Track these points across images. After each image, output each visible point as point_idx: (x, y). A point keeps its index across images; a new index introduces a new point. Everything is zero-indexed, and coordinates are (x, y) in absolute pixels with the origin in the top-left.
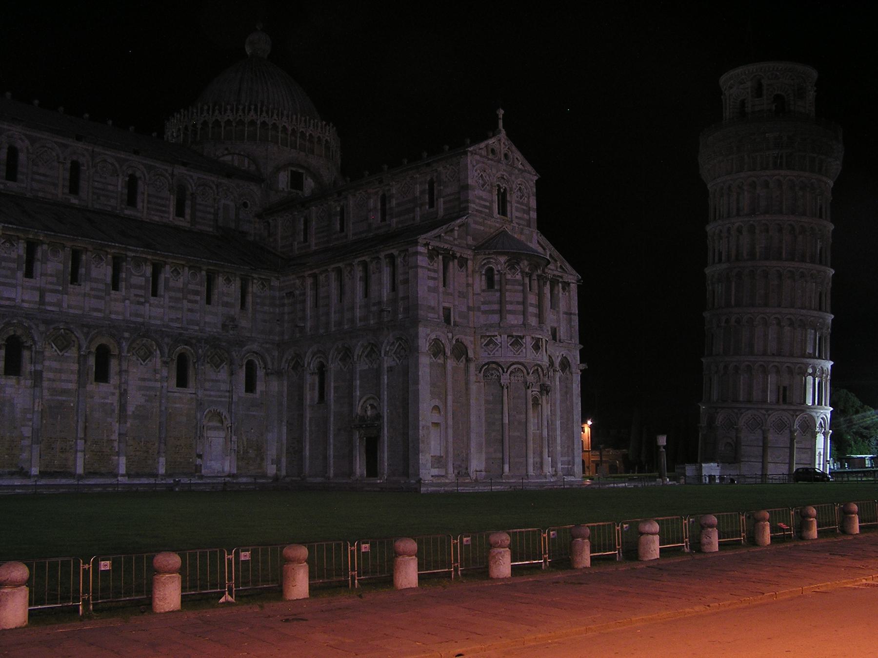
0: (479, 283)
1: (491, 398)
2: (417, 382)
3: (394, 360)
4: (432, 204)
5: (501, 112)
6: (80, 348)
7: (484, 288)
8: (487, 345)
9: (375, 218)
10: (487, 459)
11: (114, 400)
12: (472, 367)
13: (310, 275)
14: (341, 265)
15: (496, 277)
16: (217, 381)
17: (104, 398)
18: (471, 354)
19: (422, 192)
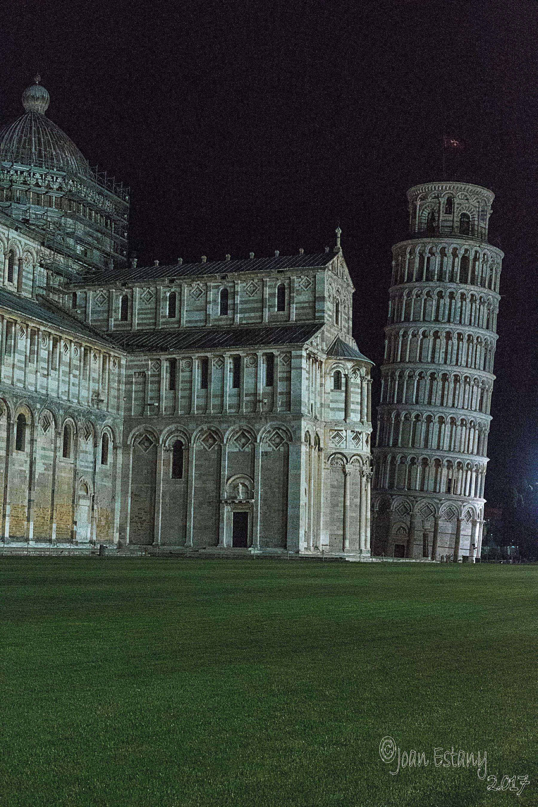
0: (330, 383)
1: (336, 483)
2: (299, 468)
3: (269, 446)
4: (281, 307)
5: (339, 231)
6: (9, 417)
7: (333, 388)
8: (334, 438)
9: (214, 311)
10: (331, 535)
11: (26, 468)
12: (323, 454)
13: (167, 359)
14: (208, 355)
15: (343, 380)
16: (86, 452)
17: (20, 466)
18: (322, 446)
19: (272, 295)
